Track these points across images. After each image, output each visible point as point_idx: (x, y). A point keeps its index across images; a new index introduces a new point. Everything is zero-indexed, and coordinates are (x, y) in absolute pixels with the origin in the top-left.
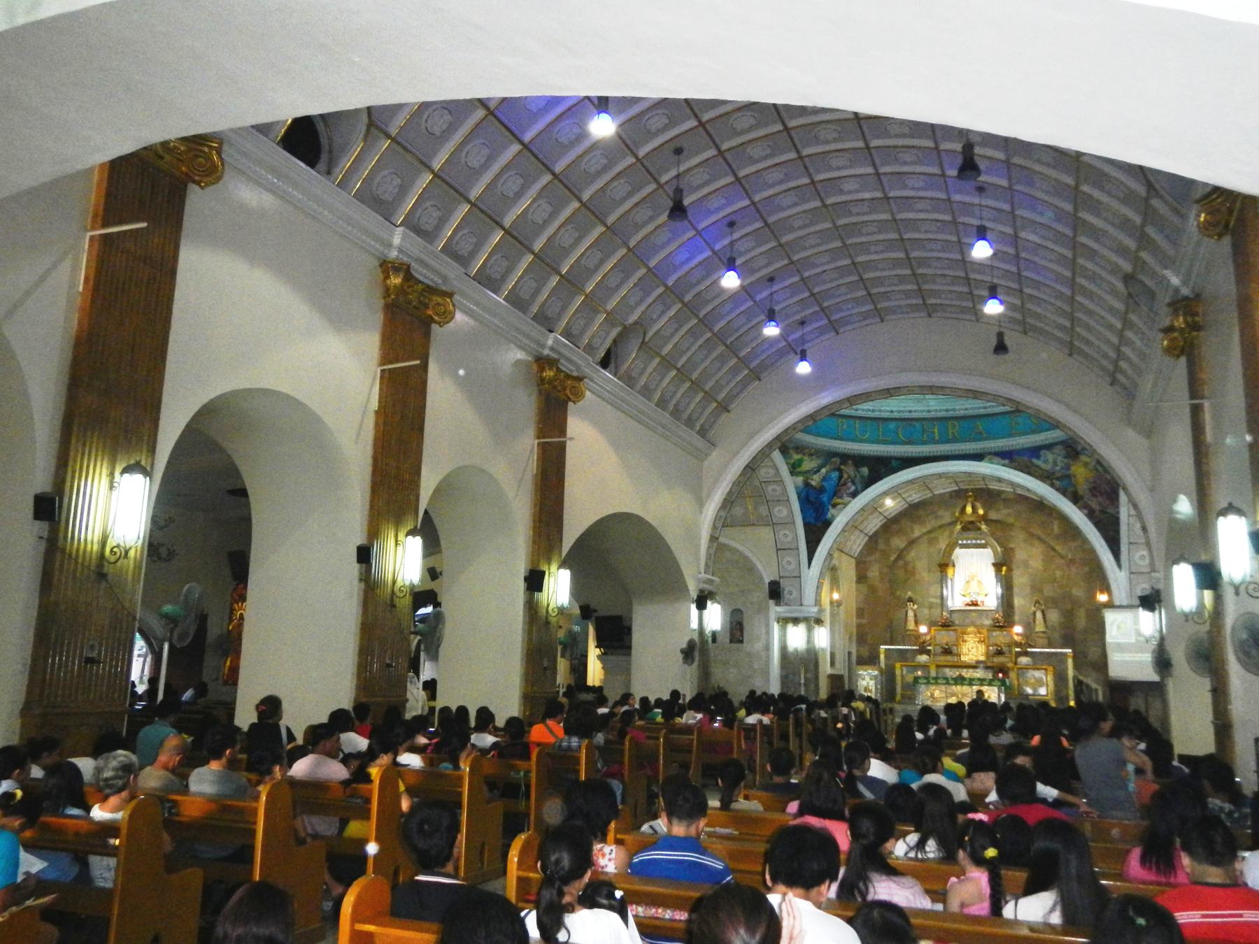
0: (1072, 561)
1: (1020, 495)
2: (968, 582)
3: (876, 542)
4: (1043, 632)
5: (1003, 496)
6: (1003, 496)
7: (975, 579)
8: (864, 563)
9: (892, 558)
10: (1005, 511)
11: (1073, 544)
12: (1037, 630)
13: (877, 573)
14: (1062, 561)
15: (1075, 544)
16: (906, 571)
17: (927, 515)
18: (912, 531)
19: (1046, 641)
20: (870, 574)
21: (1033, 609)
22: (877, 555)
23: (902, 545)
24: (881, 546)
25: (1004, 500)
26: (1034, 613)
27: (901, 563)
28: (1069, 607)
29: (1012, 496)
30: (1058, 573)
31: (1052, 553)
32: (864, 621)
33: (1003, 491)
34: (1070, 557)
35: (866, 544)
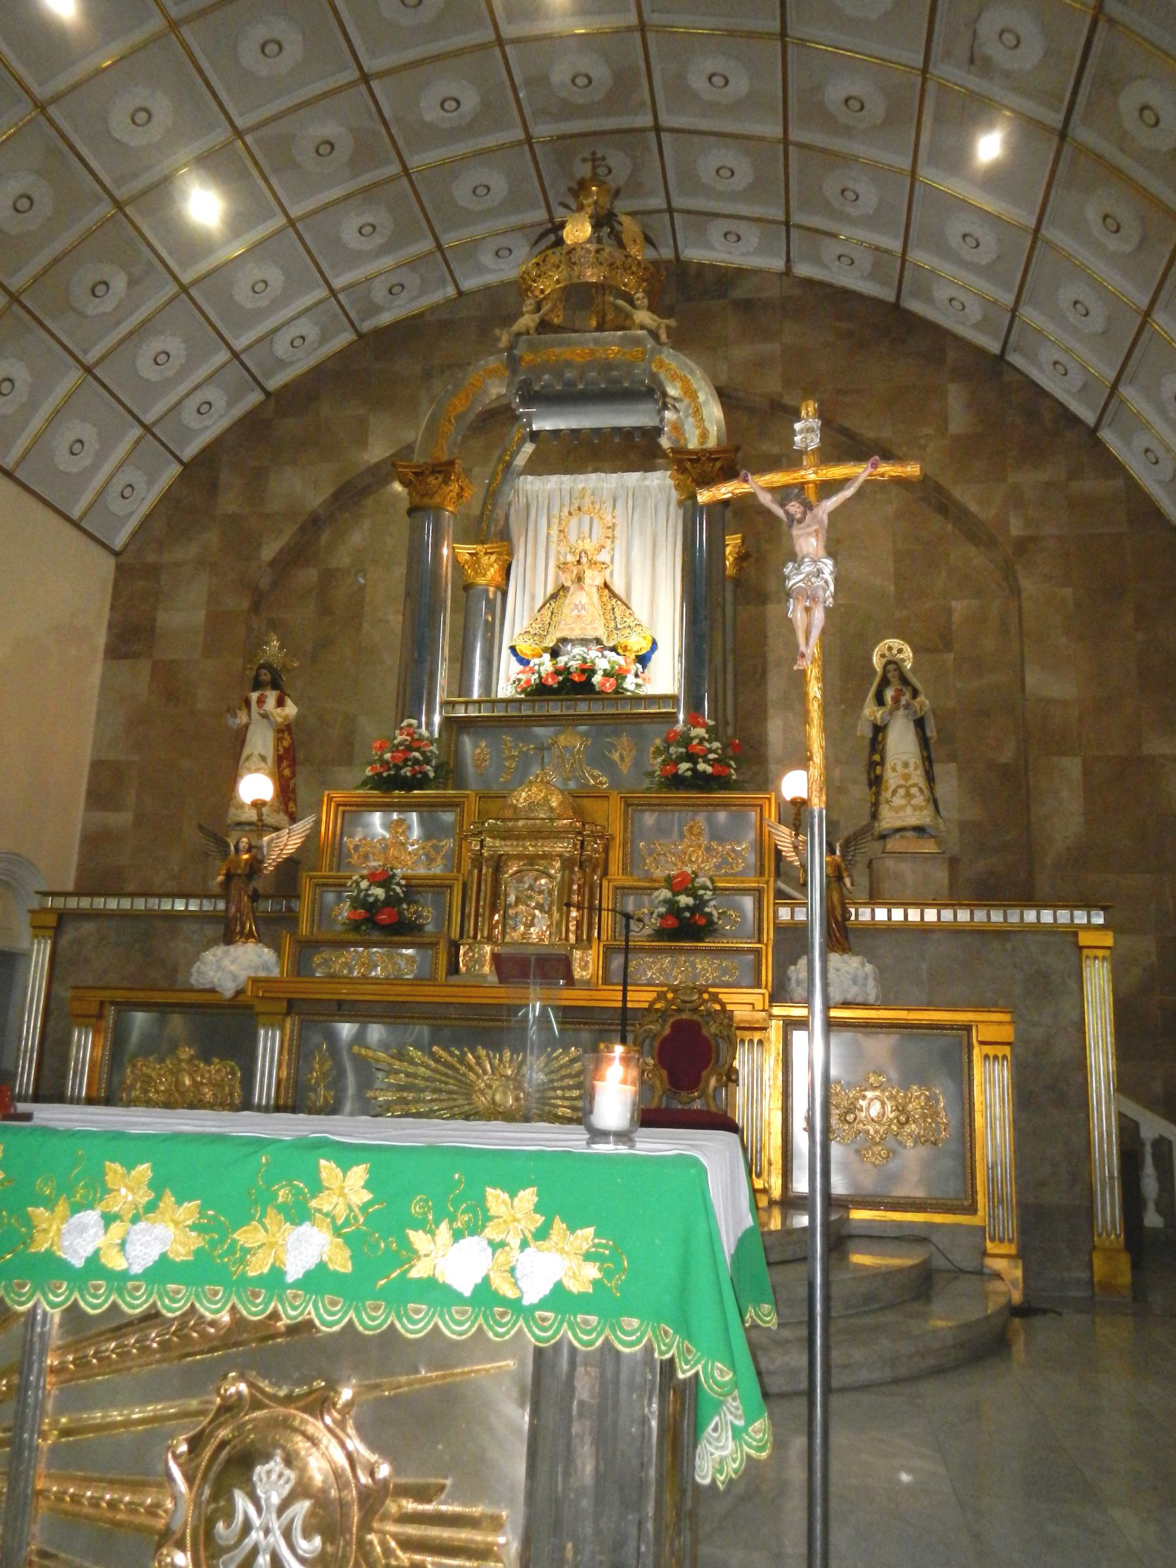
0: (1022, 546)
1: (809, 283)
2: (560, 592)
3: (213, 488)
4: (920, 830)
5: (739, 293)
6: (739, 293)
7: (593, 578)
8: (153, 571)
9: (269, 552)
10: (743, 352)
11: (1029, 479)
12: (889, 819)
13: (199, 617)
14: (977, 558)
15: (1043, 476)
16: (325, 610)
17: (428, 375)
18: (361, 441)
19: (941, 875)
20: (169, 619)
21: (870, 711)
22: (212, 537)
23: (315, 499)
24: (230, 502)
25: (747, 306)
26: (879, 730)
27: (308, 576)
28: (1007, 755)
29: (772, 292)
30: (960, 607)
31: (936, 523)
32: (122, 819)
33: (740, 272)
34: (1016, 528)
35: (167, 496)
